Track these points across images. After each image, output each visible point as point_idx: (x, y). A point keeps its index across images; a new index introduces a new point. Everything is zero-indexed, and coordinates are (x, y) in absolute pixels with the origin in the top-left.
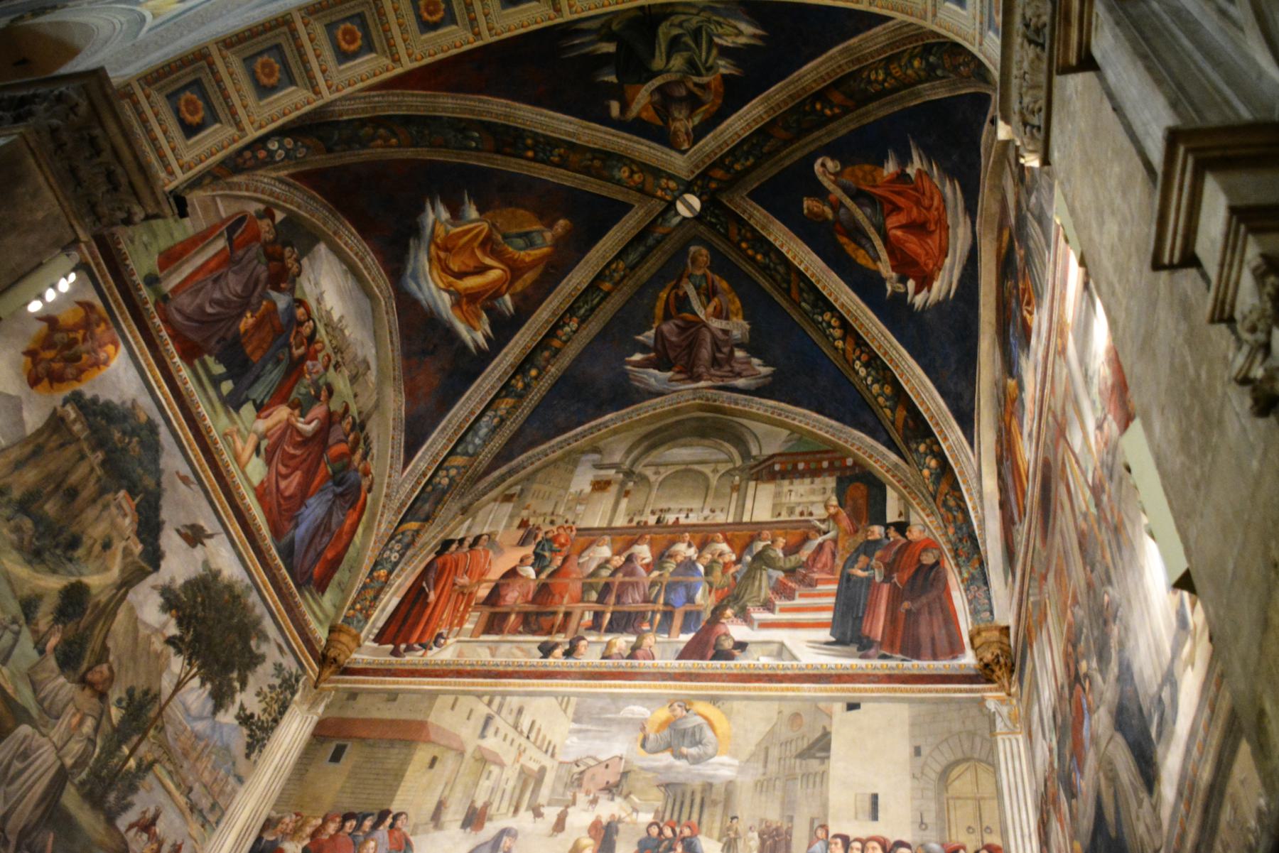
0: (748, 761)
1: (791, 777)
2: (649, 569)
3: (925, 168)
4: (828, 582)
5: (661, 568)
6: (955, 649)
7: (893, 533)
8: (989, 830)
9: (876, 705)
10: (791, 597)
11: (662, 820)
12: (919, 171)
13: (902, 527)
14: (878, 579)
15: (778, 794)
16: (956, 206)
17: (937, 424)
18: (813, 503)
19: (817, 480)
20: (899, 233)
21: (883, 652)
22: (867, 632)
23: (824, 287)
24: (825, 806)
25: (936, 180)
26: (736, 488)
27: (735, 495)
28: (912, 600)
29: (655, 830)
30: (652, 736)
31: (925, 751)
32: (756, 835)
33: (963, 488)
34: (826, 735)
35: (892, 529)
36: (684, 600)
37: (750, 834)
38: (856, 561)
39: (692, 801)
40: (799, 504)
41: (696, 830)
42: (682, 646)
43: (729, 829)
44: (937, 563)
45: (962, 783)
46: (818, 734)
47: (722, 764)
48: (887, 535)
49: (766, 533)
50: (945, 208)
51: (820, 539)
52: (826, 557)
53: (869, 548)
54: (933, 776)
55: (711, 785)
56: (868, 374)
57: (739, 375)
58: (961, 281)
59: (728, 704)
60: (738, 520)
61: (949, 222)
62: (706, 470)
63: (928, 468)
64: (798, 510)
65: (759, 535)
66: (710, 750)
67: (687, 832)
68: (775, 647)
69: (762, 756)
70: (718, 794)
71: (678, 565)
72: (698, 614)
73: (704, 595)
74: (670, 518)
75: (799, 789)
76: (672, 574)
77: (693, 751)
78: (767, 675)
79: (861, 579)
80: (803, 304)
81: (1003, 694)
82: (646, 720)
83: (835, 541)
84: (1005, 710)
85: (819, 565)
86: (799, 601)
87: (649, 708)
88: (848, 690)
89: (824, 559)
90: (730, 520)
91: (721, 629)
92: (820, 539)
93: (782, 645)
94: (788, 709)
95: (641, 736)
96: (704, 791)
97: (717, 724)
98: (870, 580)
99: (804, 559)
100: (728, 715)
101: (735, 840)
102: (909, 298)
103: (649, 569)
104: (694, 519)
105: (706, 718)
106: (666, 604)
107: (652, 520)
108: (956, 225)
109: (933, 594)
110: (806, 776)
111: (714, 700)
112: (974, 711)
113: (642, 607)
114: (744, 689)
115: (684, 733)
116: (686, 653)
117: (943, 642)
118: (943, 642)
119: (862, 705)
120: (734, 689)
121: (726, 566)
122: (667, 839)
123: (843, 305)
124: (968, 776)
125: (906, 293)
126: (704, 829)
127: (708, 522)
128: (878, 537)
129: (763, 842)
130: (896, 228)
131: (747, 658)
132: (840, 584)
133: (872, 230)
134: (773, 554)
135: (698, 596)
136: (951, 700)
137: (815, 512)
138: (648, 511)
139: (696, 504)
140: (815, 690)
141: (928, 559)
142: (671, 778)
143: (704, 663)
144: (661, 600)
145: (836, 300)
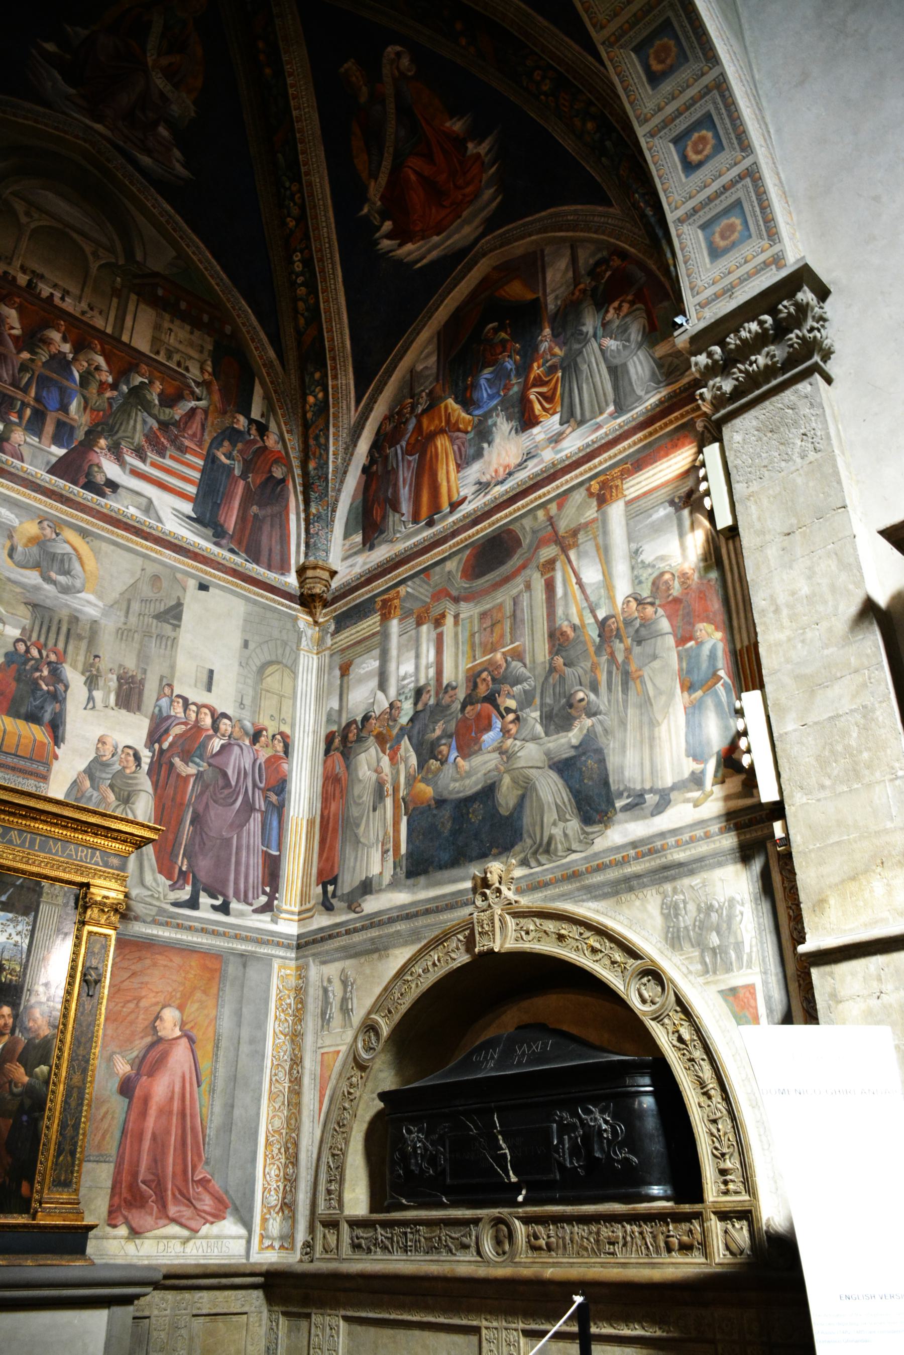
0: (112, 606)
1: (147, 634)
2: (21, 343)
3: (486, 160)
4: (195, 454)
5: (33, 352)
6: (283, 568)
7: (253, 431)
8: (284, 721)
9: (222, 593)
10: (162, 454)
11: (30, 638)
12: (478, 155)
13: (263, 429)
14: (237, 472)
15: (136, 645)
16: (484, 208)
17: (333, 359)
18: (191, 358)
19: (197, 333)
20: (413, 177)
21: (232, 546)
22: (222, 520)
23: (304, 152)
24: (173, 667)
25: (485, 177)
26: (116, 293)
27: (115, 301)
28: (261, 506)
29: (21, 647)
30: (20, 549)
31: (252, 646)
32: (115, 677)
33: (332, 430)
34: (179, 605)
35: (254, 428)
36: (58, 406)
37: (110, 676)
38: (221, 445)
39: (59, 629)
40: (178, 351)
41: (62, 657)
42: (54, 460)
43: (92, 665)
44: (283, 481)
45: (272, 680)
46: (173, 603)
47: (88, 602)
48: (249, 429)
49: (144, 368)
50: (470, 202)
51: (193, 404)
52: (196, 426)
53: (232, 435)
54: (254, 668)
55: (77, 619)
56: (302, 274)
57: (149, 152)
58: (432, 263)
59: (97, 543)
60: (116, 335)
61: (465, 214)
62: (88, 249)
63: (315, 397)
64: (176, 357)
65: (137, 365)
66: (78, 583)
67: (53, 658)
68: (144, 501)
69: (124, 606)
70: (83, 629)
71: (53, 357)
72: (72, 429)
73: (78, 410)
74: (45, 290)
75: (153, 647)
76: (44, 363)
77: (62, 579)
78: (134, 527)
79: (224, 465)
80: (280, 155)
81: (310, 619)
82: (14, 527)
83: (206, 411)
84: (309, 632)
85: (190, 432)
86: (168, 462)
87: (17, 516)
88: (202, 571)
89: (194, 426)
90: (109, 330)
91: (94, 458)
92: (193, 404)
93: (150, 501)
94: (151, 569)
95: (8, 544)
96: (70, 623)
97: (85, 559)
98: (230, 469)
99: (177, 417)
100: (96, 553)
101: (97, 676)
102: (378, 235)
103: (21, 343)
104: (68, 305)
105: (75, 549)
106: (37, 399)
107: (22, 279)
108: (467, 222)
109: (276, 509)
110: (160, 637)
111: (84, 533)
112: (289, 625)
113: (11, 391)
114: (113, 533)
115: (53, 557)
116: (58, 469)
117: (276, 558)
118: (276, 558)
119: (211, 589)
120: (103, 529)
121: (102, 386)
122: (33, 658)
123: (310, 184)
124: (277, 676)
125: (378, 228)
126: (69, 660)
127: (84, 318)
128: (242, 428)
129: (120, 686)
130: (416, 172)
131: (117, 501)
132: (206, 461)
133: (391, 150)
134: (149, 397)
135: (73, 407)
136: (275, 610)
137: (191, 368)
138: (17, 264)
139: (75, 290)
140: (175, 560)
141: (278, 473)
142: (36, 599)
143: (77, 489)
144: (33, 394)
145: (307, 174)
